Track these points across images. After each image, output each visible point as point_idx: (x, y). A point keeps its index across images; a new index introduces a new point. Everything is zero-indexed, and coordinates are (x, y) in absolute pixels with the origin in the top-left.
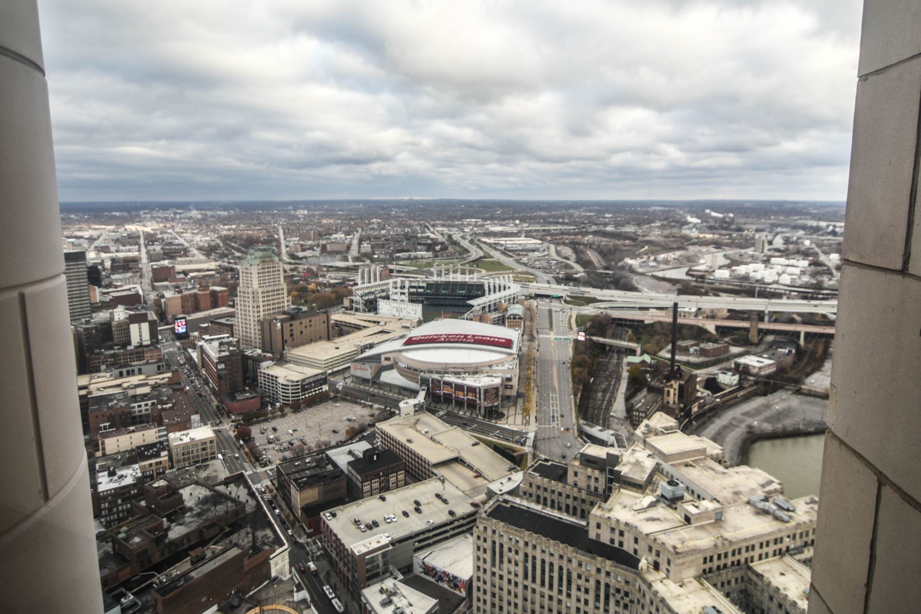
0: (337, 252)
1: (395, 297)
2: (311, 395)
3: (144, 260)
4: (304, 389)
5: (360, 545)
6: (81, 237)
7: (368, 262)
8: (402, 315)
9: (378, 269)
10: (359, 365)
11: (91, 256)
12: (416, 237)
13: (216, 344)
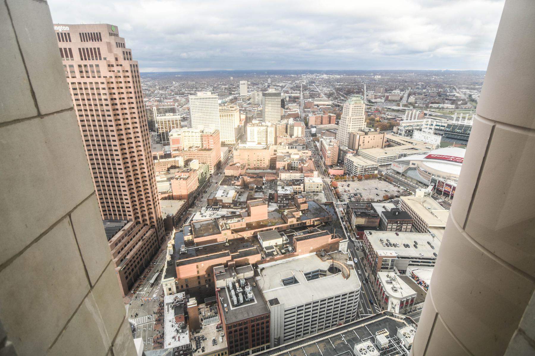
0: (394, 101)
1: (425, 130)
2: (367, 175)
3: (302, 98)
4: (365, 170)
5: (382, 252)
6: (279, 86)
7: (411, 108)
8: (427, 141)
9: (418, 112)
10: (396, 164)
11: (282, 94)
12: (446, 95)
13: (328, 141)
